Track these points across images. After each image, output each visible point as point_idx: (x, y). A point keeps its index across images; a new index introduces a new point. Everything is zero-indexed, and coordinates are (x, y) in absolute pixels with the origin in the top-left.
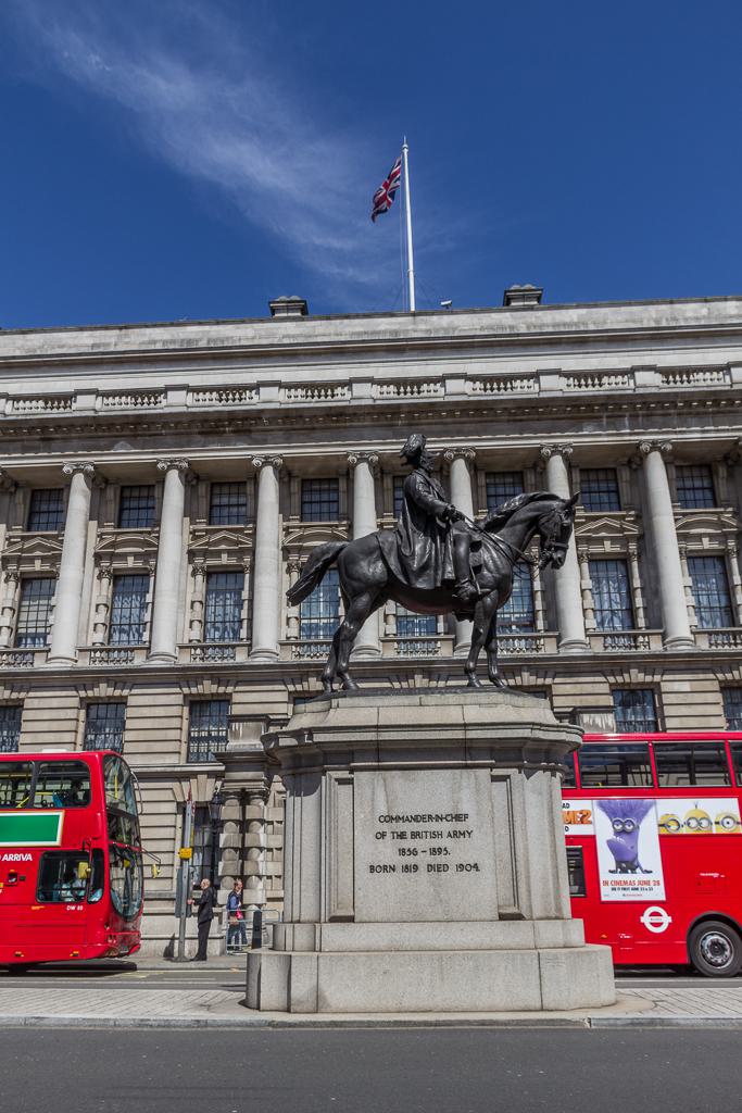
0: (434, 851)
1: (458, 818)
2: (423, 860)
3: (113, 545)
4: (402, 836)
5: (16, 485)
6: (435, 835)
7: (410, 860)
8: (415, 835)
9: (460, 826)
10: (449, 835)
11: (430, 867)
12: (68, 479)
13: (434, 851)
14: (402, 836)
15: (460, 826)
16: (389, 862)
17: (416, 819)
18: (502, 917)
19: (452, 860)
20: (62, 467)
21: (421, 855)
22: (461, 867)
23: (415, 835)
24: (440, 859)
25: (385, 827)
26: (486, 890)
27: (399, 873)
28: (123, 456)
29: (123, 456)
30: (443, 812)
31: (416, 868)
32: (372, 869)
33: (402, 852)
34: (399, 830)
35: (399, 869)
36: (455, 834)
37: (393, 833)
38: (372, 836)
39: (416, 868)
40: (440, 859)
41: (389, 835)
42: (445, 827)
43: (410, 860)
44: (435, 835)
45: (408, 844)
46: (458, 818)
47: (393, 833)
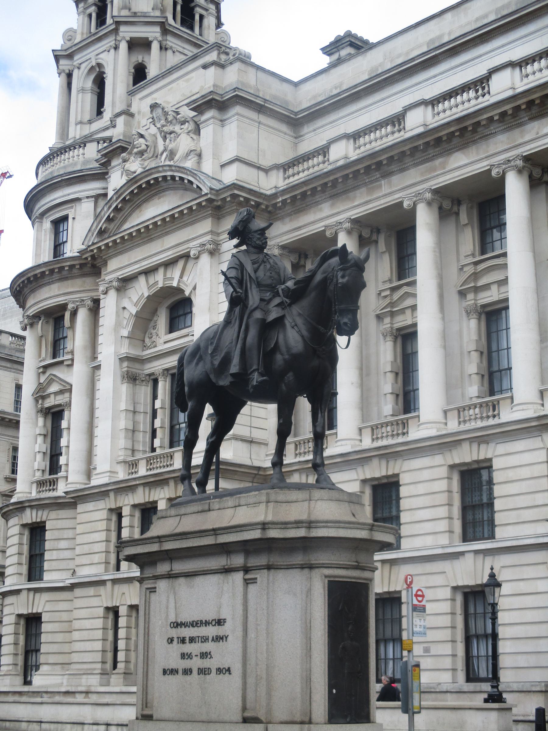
1: (220, 622)
2: (196, 663)
3: (476, 276)
4: (183, 641)
6: (205, 639)
8: (192, 640)
10: (213, 640)
11: (203, 671)
13: (204, 655)
14: (183, 641)
16: (173, 666)
17: (194, 624)
18: (245, 720)
20: (401, 203)
21: (195, 658)
22: (219, 671)
23: (192, 640)
27: (180, 677)
28: (462, 166)
29: (462, 166)
30: (209, 618)
31: (191, 671)
32: (165, 672)
34: (182, 635)
35: (180, 672)
36: (219, 639)
37: (178, 638)
38: (165, 641)
39: (191, 671)
40: (206, 663)
41: (176, 640)
42: (211, 631)
44: (205, 639)
45: (188, 648)
46: (220, 622)
47: (178, 638)
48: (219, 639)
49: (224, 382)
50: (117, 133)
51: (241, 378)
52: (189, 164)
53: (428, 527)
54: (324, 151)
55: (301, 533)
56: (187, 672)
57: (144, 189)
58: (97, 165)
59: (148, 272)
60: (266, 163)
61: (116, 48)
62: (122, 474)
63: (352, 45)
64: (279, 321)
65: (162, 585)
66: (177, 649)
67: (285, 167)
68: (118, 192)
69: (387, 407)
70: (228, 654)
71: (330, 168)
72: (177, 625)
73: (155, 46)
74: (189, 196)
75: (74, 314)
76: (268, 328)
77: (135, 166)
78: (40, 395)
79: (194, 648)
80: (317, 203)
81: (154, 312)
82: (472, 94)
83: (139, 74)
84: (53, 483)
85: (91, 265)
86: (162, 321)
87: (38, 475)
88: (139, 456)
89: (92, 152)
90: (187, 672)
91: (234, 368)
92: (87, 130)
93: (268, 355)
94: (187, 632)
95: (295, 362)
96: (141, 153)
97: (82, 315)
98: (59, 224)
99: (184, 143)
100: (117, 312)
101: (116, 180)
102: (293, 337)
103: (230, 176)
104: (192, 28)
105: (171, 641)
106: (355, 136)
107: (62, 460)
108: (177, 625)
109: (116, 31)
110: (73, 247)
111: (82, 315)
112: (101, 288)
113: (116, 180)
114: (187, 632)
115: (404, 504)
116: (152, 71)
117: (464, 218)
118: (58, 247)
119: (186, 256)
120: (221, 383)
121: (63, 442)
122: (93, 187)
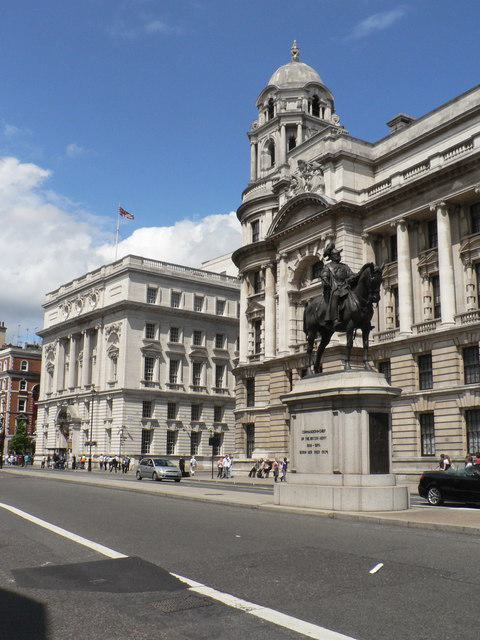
0: (317, 445)
1: (323, 431)
2: (313, 449)
5: (418, 223)
7: (310, 449)
8: (312, 438)
9: (322, 435)
11: (316, 452)
12: (434, 213)
13: (317, 445)
15: (322, 435)
18: (335, 473)
19: (320, 449)
24: (317, 449)
25: (304, 436)
26: (327, 462)
33: (308, 446)
36: (322, 438)
40: (317, 449)
42: (319, 435)
43: (310, 449)
45: (310, 442)
46: (323, 431)
48: (322, 438)
49: (323, 324)
50: (283, 175)
51: (330, 322)
52: (319, 192)
53: (447, 377)
54: (388, 181)
55: (355, 392)
56: (310, 452)
57: (296, 206)
58: (271, 193)
59: (300, 249)
60: (359, 189)
61: (279, 130)
62: (292, 353)
63: (403, 120)
64: (346, 296)
65: (298, 415)
66: (306, 442)
67: (368, 191)
68: (284, 207)
69: (427, 315)
70: (325, 445)
71: (391, 191)
72: (306, 432)
73: (300, 127)
74: (320, 208)
75: (264, 271)
76: (341, 300)
77: (292, 194)
78: (249, 314)
79: (312, 442)
80: (385, 209)
81: (305, 269)
82: (464, 148)
83: (292, 142)
84: (258, 357)
85: (270, 247)
86: (309, 273)
87: (250, 354)
88: (299, 343)
89: (269, 185)
90: (310, 452)
91: (327, 318)
92: (267, 174)
93: (342, 312)
94: (309, 435)
95: (353, 315)
96: (294, 187)
97: (269, 271)
98: (255, 225)
99: (315, 181)
100: (286, 270)
101: (283, 201)
102: (353, 302)
103: (340, 197)
104: (318, 115)
105: (303, 439)
106: (404, 173)
107: (262, 346)
108: (306, 432)
109: (278, 121)
110: (263, 236)
111: (268, 271)
112: (278, 258)
113: (283, 201)
114: (309, 435)
115: (434, 366)
116: (299, 141)
117: (462, 213)
118: (255, 235)
119: (319, 240)
120: (321, 324)
121: (262, 336)
122: (271, 205)
